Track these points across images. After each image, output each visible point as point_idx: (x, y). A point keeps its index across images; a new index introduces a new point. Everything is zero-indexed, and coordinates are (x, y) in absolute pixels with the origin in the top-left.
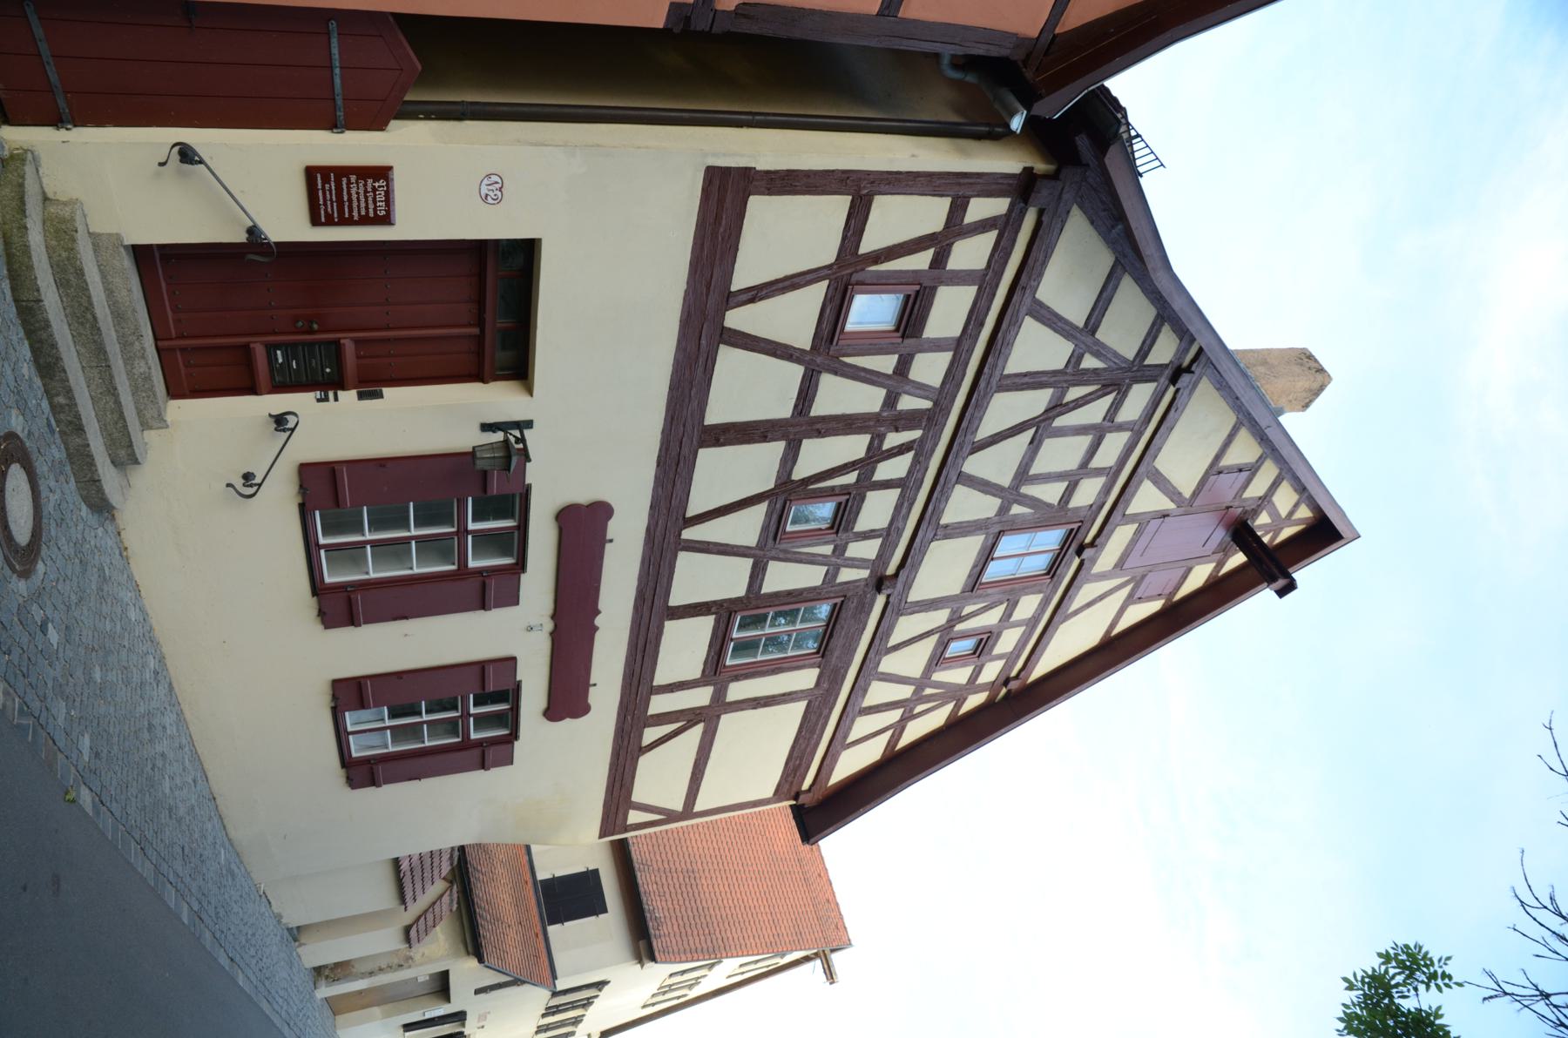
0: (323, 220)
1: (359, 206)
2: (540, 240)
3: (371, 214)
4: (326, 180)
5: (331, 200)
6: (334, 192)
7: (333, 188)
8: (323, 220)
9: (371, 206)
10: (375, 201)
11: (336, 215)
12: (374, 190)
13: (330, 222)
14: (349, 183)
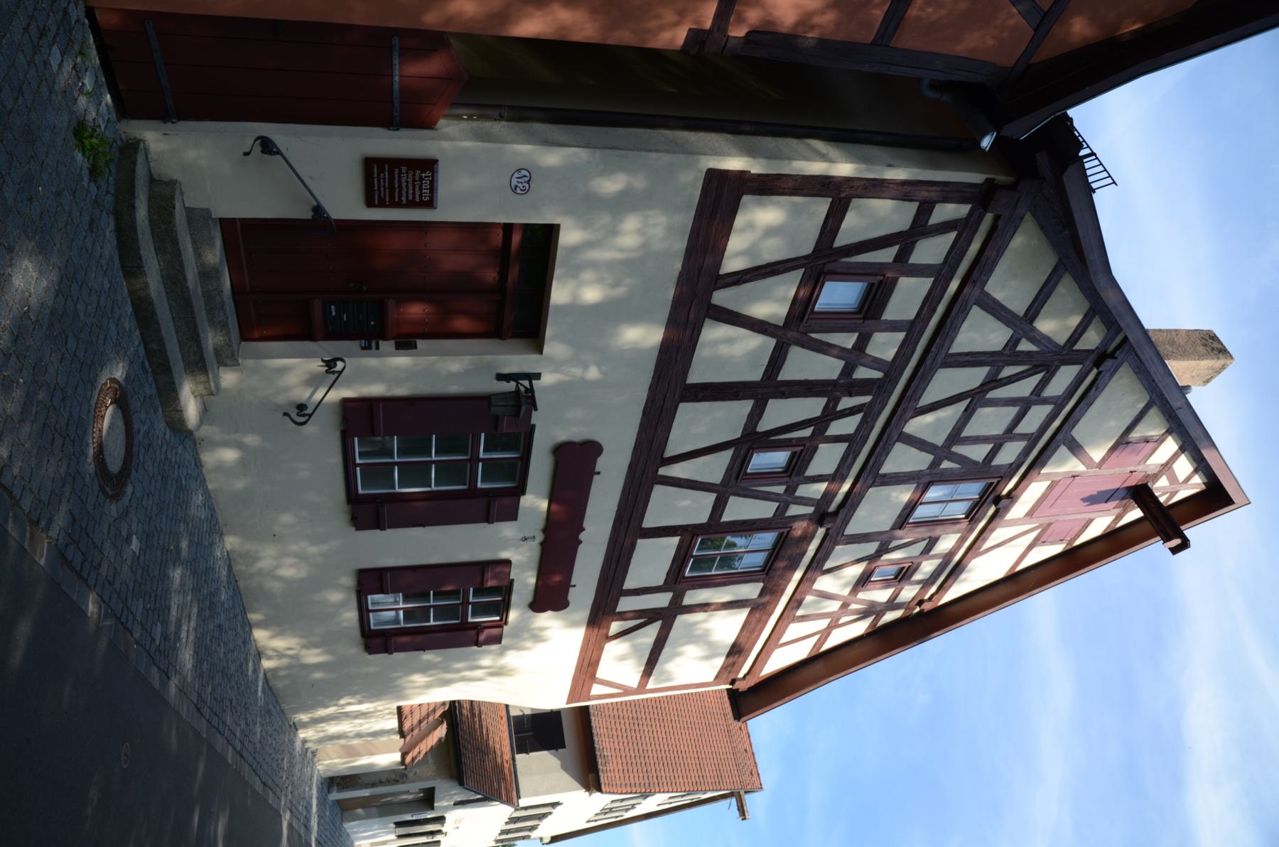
0: (376, 202)
1: (407, 193)
3: (417, 200)
4: (381, 170)
6: (387, 180)
7: (387, 176)
8: (376, 202)
9: (418, 193)
10: (421, 189)
11: (387, 199)
13: (382, 204)
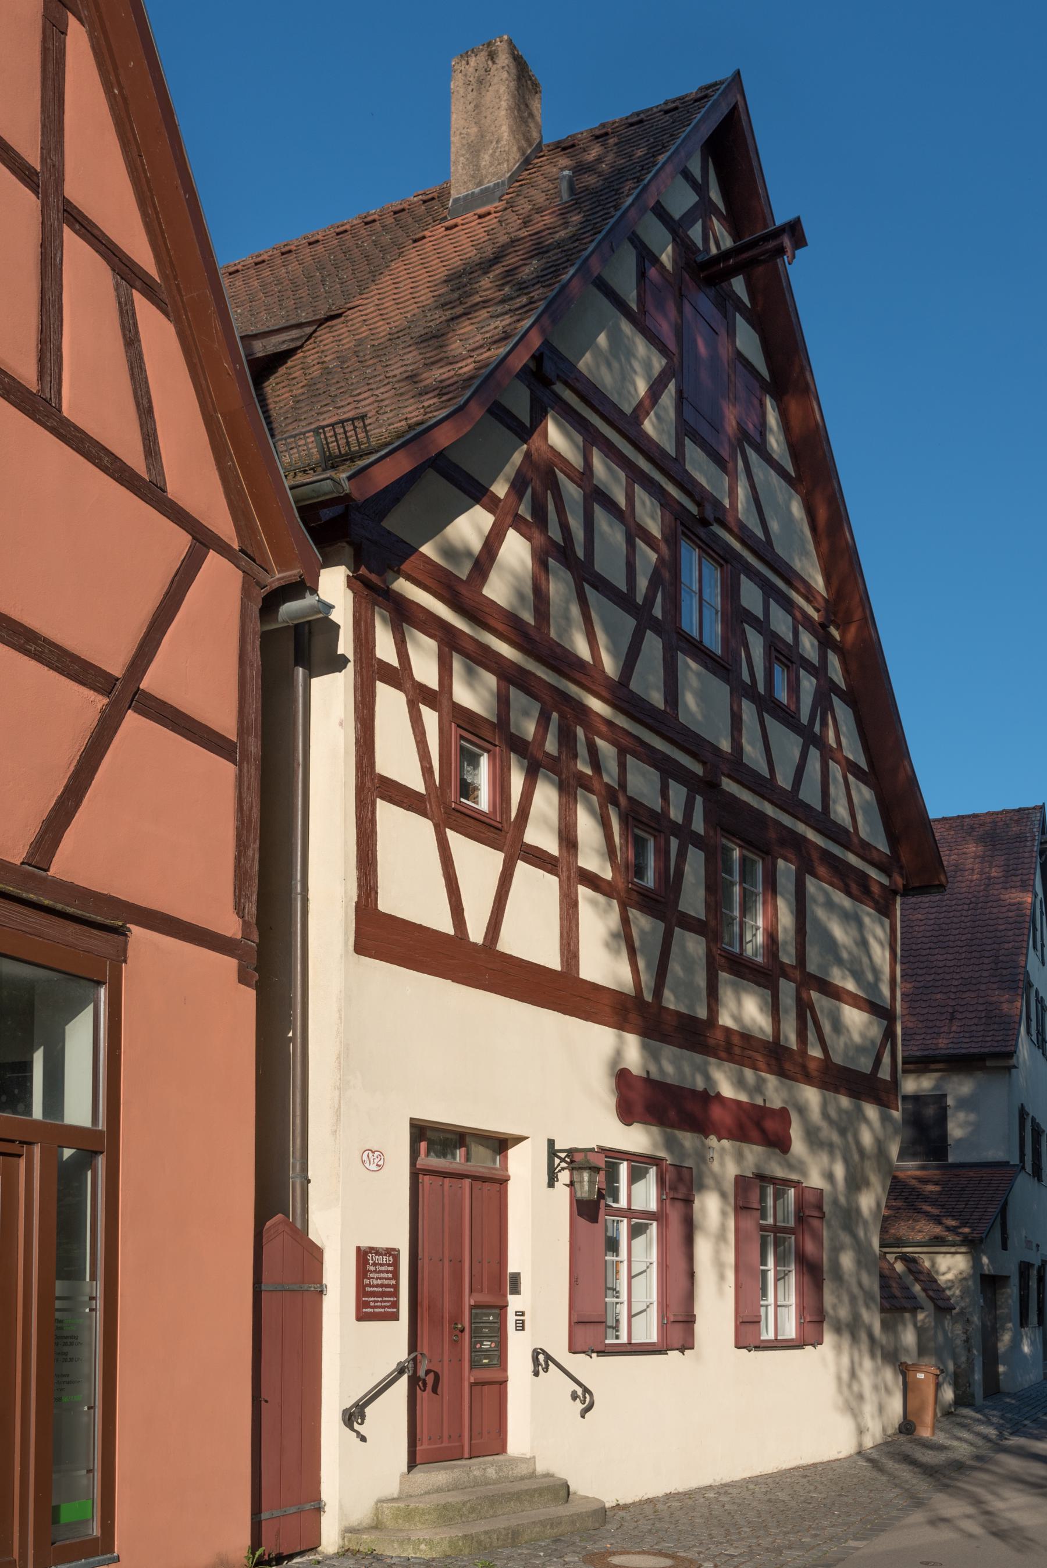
0: (395, 1310)
1: (386, 1279)
2: (411, 1119)
3: (391, 1268)
4: (367, 1305)
5: (381, 1302)
6: (376, 1299)
7: (373, 1299)
8: (395, 1310)
9: (386, 1268)
10: (382, 1265)
11: (392, 1299)
12: (374, 1264)
13: (396, 1305)
14: (369, 1285)
